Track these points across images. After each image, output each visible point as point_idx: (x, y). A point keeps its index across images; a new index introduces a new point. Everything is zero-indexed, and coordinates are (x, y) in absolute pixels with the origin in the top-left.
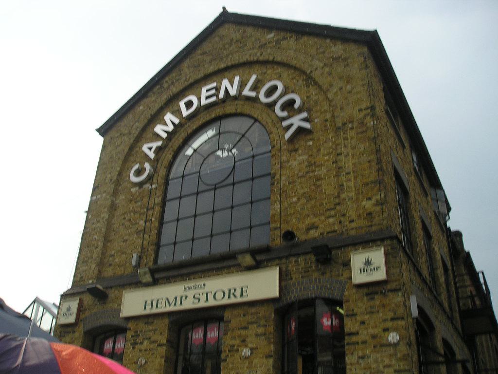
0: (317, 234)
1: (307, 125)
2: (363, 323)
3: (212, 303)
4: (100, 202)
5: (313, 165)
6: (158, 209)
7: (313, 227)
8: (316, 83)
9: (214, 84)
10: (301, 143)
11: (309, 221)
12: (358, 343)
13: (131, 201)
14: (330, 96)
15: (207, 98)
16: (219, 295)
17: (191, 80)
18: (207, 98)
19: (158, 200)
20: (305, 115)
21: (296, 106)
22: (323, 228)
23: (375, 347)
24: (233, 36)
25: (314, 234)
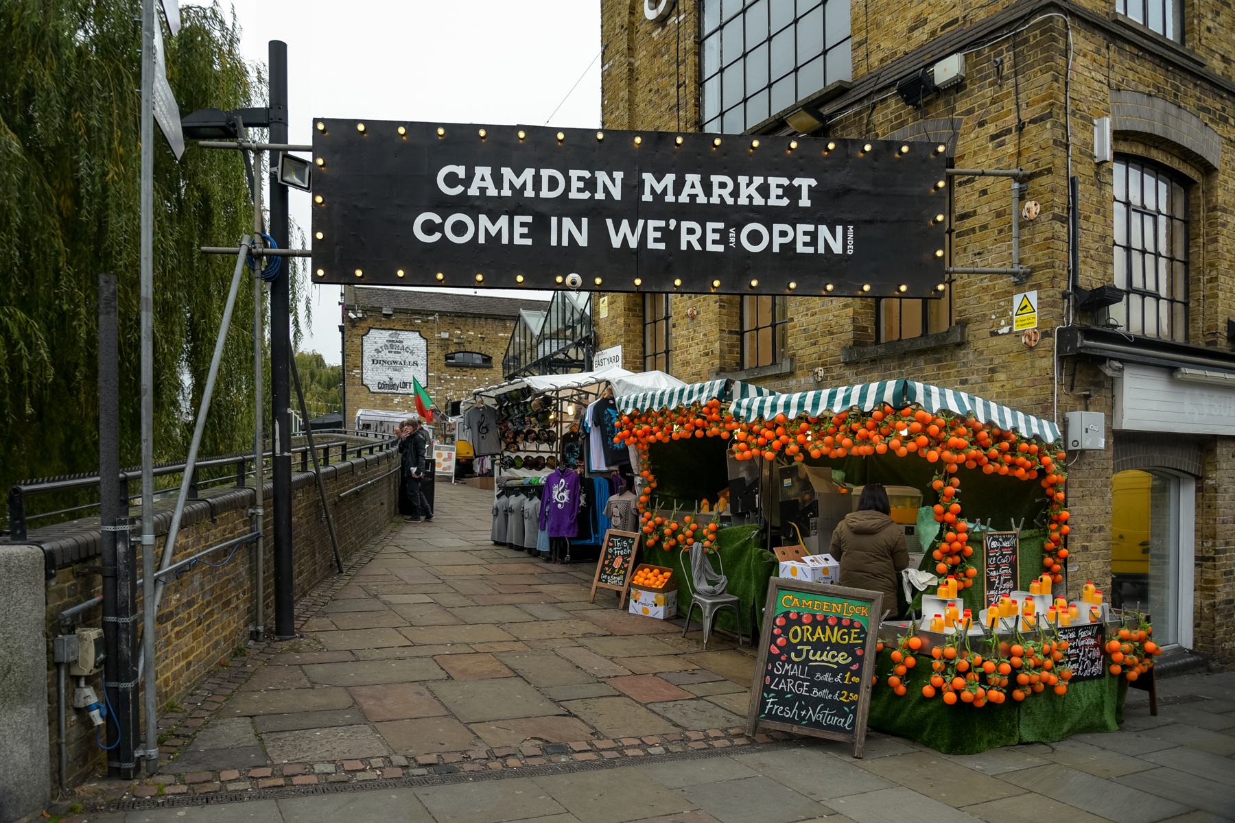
0: (925, 37)
2: (984, 192)
4: (615, 72)
6: (691, 59)
7: (919, 22)
11: (911, 14)
12: (973, 230)
13: (655, 56)
19: (689, 43)
23: (1000, 231)
25: (921, 35)
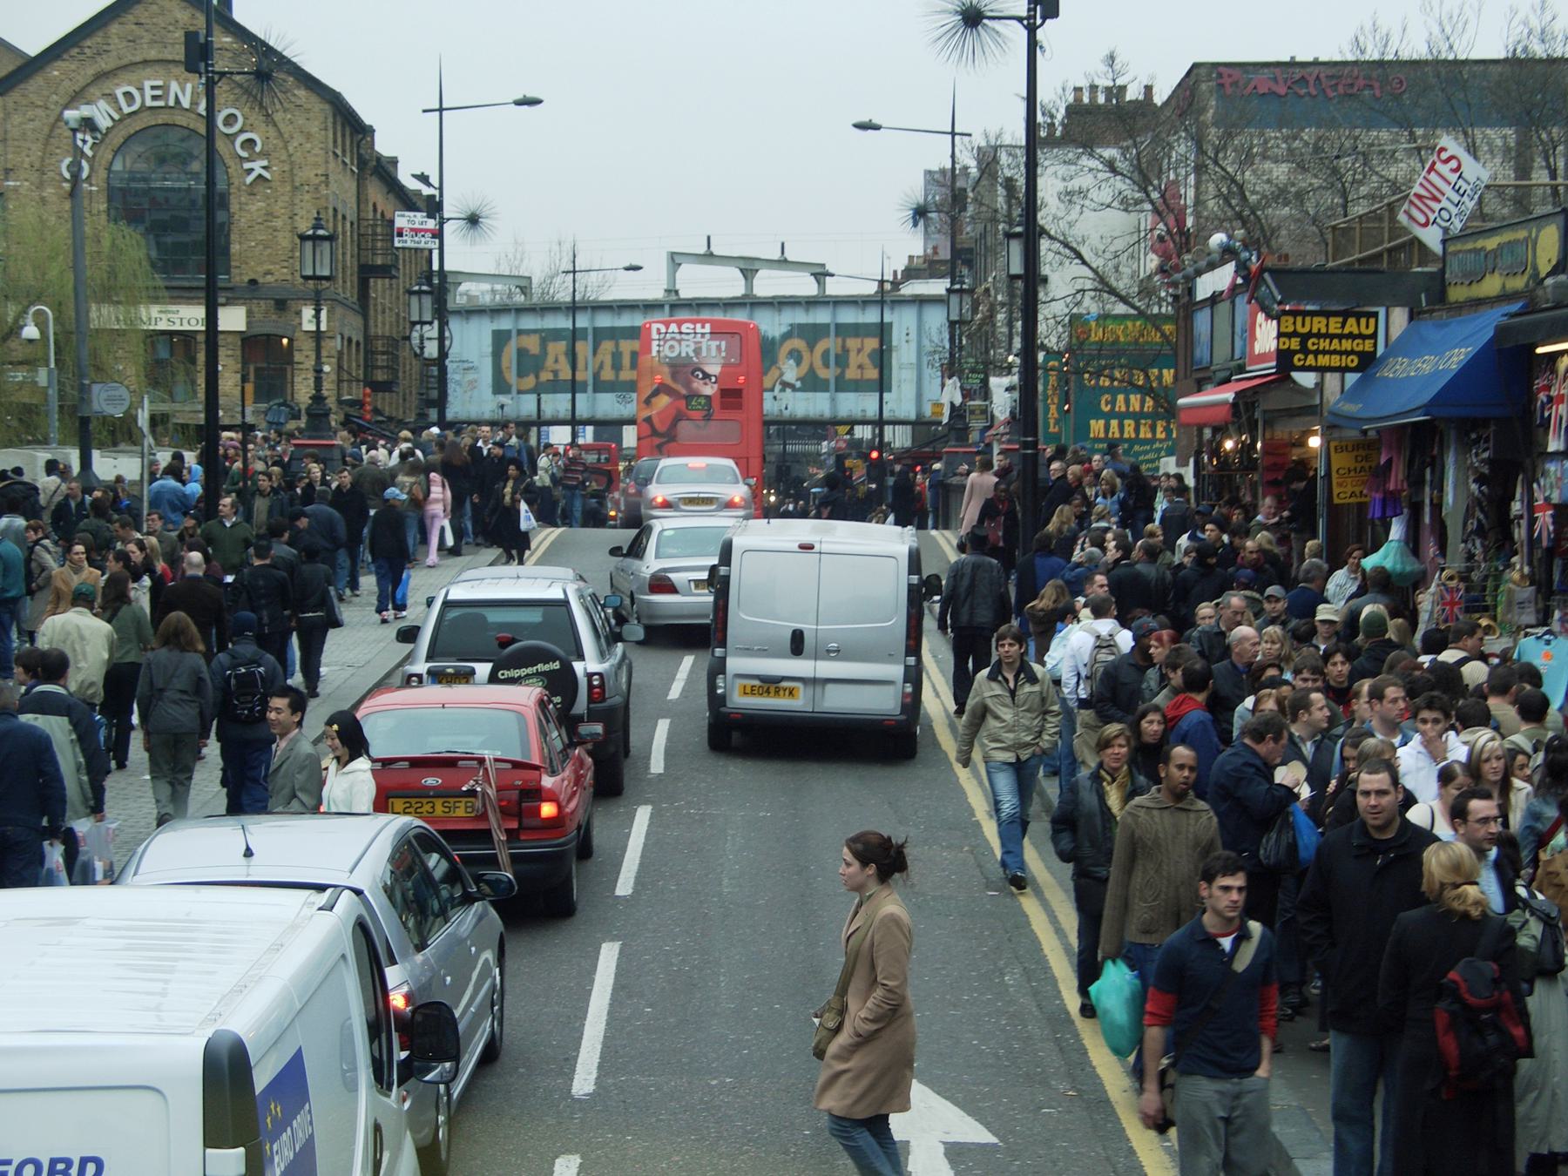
1: (266, 175)
3: (186, 327)
5: (270, 215)
8: (275, 125)
9: (160, 83)
10: (259, 188)
14: (291, 149)
15: (154, 98)
16: (193, 322)
17: (125, 61)
18: (154, 98)
20: (265, 163)
21: (258, 149)
22: (277, 276)
24: (179, 16)
25: (269, 278)
